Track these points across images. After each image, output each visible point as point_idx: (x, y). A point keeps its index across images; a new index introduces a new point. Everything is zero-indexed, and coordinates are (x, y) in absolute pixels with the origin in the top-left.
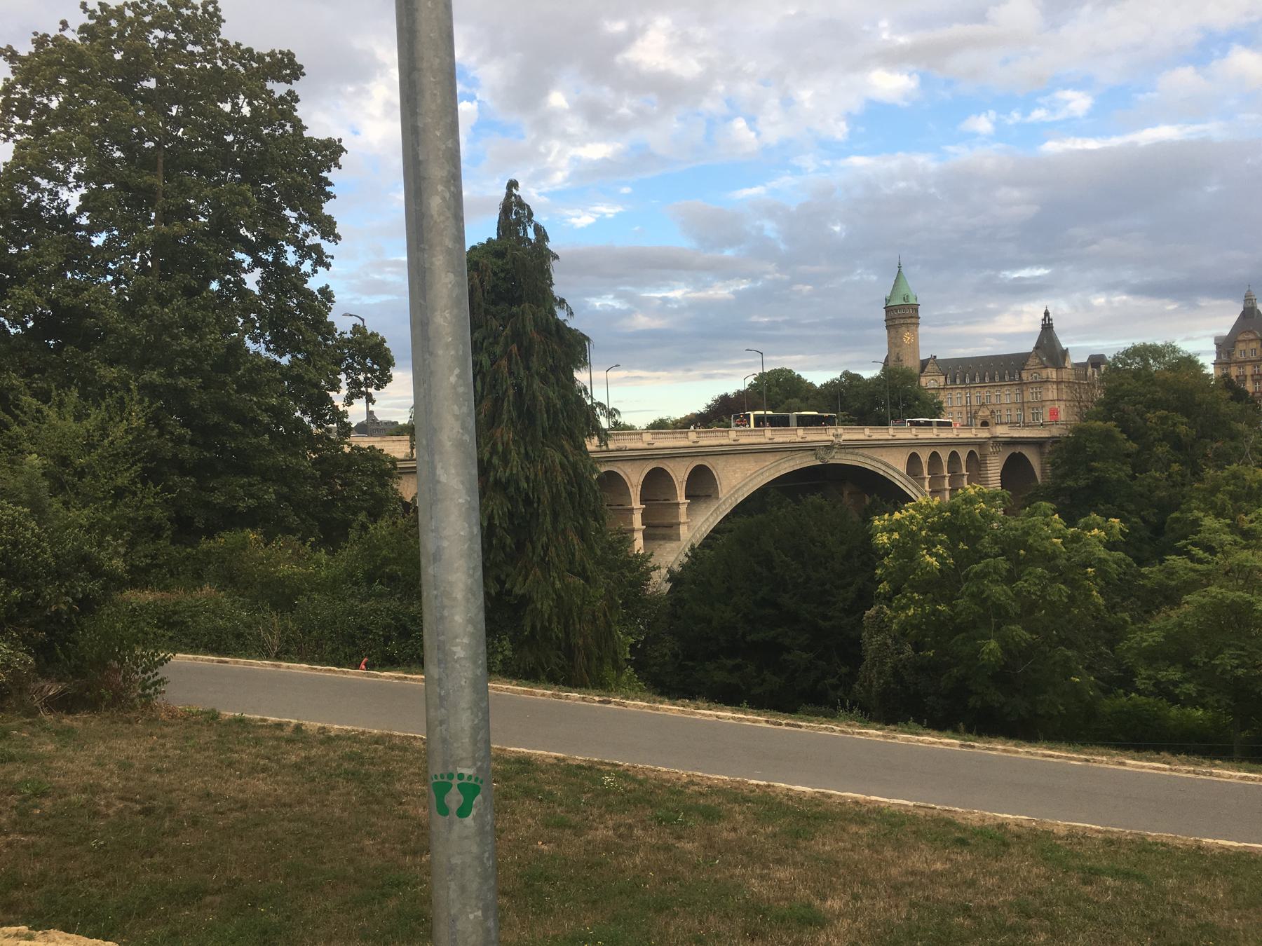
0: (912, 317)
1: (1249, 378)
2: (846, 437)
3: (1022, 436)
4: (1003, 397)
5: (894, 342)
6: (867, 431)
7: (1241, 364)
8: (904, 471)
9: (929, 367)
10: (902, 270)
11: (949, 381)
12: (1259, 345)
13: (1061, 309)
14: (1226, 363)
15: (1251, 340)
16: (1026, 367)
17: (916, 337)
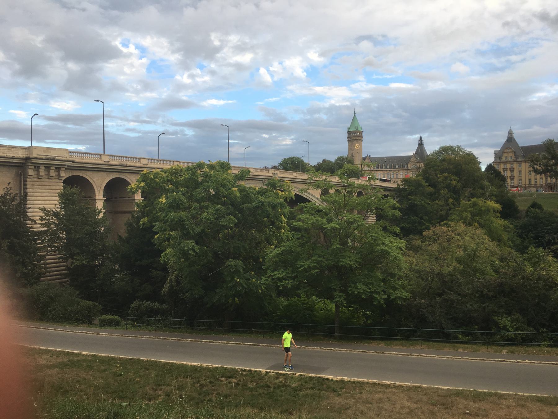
0: (359, 137)
1: (508, 170)
2: (282, 176)
3: (388, 186)
4: (399, 175)
5: (351, 148)
6: (295, 174)
7: (505, 163)
8: (319, 197)
10: (356, 115)
11: (375, 168)
12: (513, 154)
13: (425, 136)
14: (499, 163)
15: (510, 152)
16: (410, 162)
17: (361, 146)
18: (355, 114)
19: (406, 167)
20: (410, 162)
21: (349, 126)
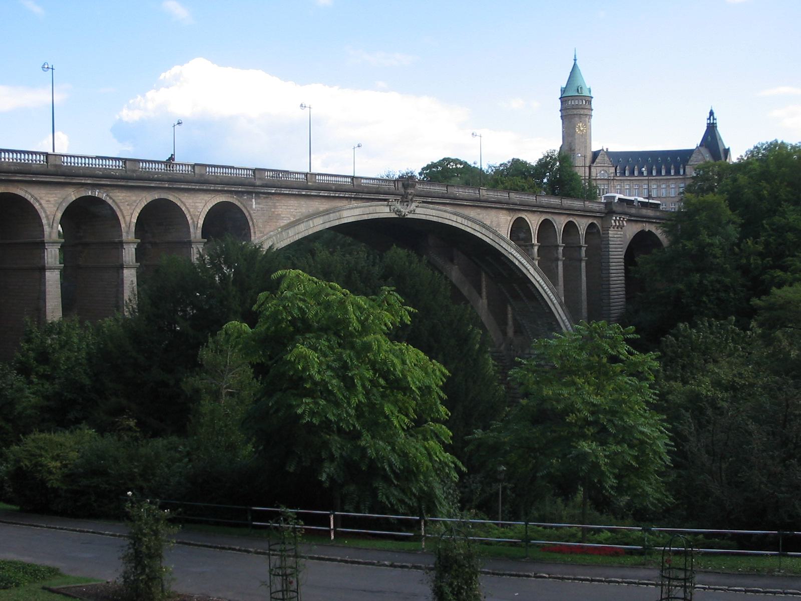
9: (599, 157)
10: (577, 62)
18: (575, 60)
19: (682, 172)
20: (690, 163)
21: (564, 86)
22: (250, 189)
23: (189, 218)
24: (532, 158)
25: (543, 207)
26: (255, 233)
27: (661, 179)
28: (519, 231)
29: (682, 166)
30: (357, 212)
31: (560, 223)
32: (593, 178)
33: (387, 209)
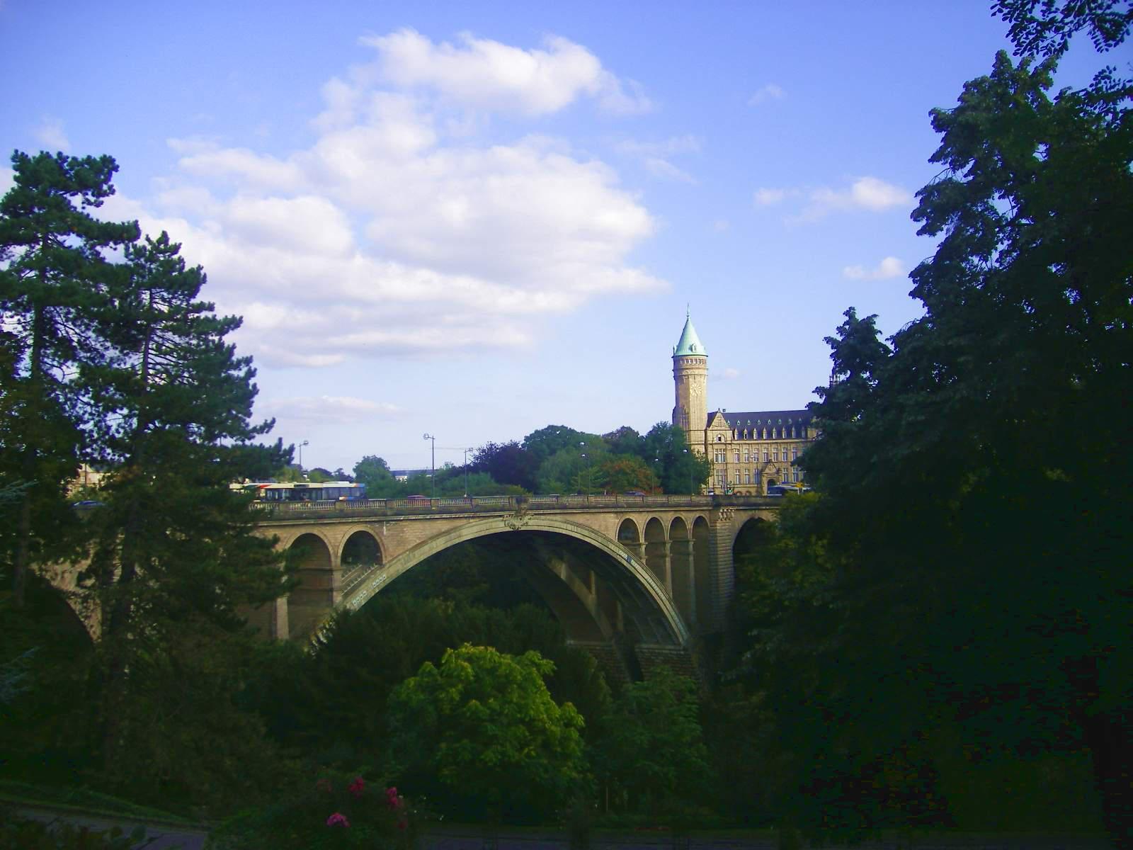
19: (803, 434)
22: (382, 518)
23: (330, 549)
24: (643, 429)
25: (649, 507)
26: (386, 557)
27: (782, 443)
28: (627, 531)
29: (803, 428)
30: (475, 529)
31: (667, 519)
32: (709, 442)
33: (502, 524)
